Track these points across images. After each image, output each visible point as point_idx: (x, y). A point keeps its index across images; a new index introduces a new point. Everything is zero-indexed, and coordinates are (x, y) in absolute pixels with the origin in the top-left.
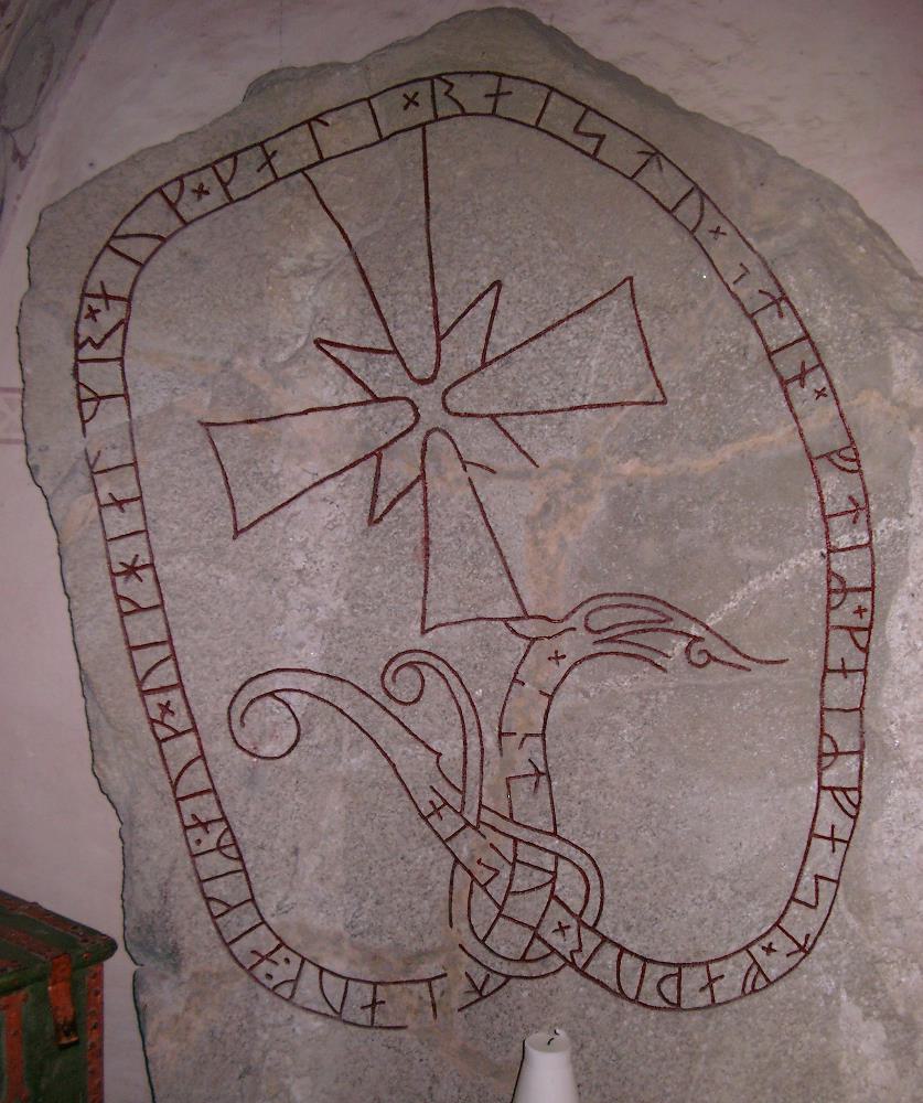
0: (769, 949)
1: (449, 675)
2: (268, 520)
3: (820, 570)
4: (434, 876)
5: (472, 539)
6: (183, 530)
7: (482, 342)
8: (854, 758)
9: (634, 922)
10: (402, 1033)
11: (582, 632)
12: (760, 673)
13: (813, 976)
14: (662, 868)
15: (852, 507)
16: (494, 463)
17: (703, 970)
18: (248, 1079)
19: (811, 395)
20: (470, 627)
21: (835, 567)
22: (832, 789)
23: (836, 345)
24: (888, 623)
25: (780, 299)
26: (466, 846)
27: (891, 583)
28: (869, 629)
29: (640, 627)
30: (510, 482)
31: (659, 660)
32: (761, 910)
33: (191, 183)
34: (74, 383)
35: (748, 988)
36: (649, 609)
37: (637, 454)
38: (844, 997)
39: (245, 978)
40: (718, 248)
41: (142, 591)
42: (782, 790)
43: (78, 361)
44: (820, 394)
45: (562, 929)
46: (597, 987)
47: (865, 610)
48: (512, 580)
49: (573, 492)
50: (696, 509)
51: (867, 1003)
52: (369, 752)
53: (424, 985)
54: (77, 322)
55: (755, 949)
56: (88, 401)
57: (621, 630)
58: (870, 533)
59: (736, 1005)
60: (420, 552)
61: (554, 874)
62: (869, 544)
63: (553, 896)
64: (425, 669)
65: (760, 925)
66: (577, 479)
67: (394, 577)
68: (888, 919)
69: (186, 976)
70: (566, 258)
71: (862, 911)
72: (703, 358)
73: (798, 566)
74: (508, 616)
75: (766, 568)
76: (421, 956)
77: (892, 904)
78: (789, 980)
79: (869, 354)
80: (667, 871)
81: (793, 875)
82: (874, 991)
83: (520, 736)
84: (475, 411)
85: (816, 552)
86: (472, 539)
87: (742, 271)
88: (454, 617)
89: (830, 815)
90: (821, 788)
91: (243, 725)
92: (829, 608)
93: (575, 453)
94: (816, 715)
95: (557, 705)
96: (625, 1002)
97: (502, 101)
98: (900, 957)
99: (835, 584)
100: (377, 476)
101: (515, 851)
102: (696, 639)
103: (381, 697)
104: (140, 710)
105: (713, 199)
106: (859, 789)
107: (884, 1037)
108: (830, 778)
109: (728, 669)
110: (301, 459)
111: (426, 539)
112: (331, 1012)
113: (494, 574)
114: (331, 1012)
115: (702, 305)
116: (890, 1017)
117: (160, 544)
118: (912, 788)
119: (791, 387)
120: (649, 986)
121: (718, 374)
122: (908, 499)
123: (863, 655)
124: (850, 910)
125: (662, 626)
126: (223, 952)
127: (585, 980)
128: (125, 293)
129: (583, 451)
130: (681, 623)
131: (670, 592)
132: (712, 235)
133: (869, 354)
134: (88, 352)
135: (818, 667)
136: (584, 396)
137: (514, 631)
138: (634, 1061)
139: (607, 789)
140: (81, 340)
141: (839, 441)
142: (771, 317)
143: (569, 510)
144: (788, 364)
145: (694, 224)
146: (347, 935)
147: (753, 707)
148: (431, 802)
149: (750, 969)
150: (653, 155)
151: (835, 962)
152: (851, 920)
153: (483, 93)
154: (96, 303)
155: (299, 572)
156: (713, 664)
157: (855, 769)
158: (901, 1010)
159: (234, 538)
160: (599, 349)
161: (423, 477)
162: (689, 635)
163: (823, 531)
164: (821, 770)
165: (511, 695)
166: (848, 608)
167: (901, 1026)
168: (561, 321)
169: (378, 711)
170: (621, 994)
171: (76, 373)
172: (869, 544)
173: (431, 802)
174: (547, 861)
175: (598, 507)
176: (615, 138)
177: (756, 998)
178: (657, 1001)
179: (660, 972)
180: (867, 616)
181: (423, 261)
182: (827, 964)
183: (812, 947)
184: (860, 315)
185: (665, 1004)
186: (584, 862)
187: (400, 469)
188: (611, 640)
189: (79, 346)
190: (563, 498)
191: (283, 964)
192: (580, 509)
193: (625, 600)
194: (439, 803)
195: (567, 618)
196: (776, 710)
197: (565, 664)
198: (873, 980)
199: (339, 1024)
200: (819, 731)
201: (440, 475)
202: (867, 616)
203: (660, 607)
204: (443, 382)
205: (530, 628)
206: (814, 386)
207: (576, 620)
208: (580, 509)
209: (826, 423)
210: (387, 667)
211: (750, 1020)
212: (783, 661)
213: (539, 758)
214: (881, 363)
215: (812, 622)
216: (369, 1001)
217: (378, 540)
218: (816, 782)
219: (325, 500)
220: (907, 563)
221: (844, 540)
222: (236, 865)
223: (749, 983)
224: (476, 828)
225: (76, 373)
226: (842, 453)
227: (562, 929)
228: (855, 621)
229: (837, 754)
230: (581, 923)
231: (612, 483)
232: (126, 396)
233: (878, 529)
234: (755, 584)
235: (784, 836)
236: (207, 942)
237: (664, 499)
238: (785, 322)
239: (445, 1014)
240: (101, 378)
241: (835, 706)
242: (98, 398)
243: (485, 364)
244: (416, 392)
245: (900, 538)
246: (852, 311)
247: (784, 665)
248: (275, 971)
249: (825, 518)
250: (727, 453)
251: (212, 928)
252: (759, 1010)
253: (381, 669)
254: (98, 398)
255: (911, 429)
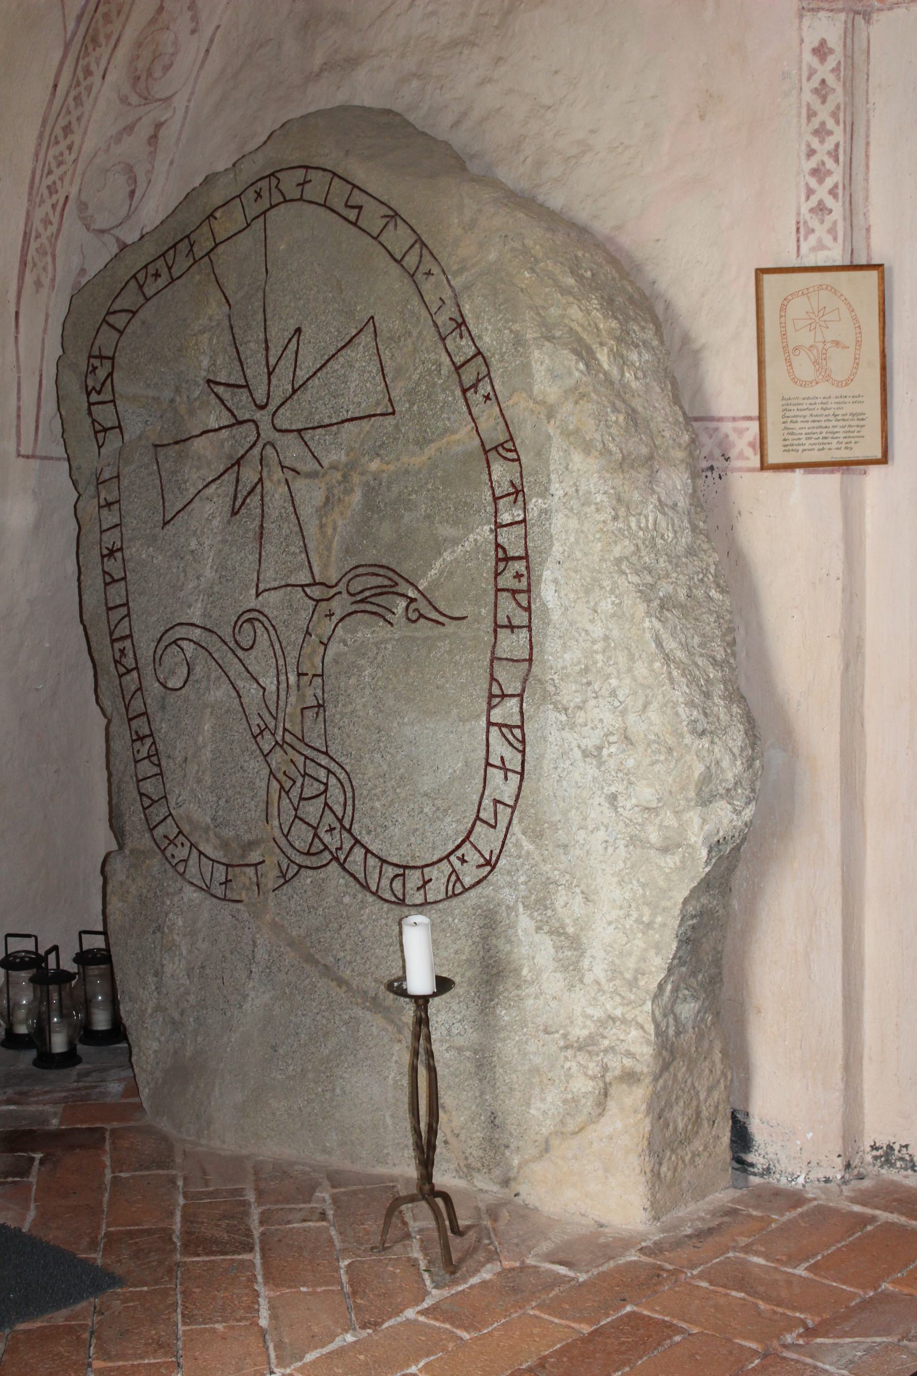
0: (463, 860)
1: (270, 628)
2: (181, 515)
3: (490, 543)
4: (258, 783)
5: (286, 525)
6: (137, 523)
7: (291, 375)
8: (515, 701)
9: (372, 827)
10: (239, 906)
11: (345, 595)
12: (451, 627)
13: (498, 889)
14: (389, 785)
15: (512, 490)
16: (299, 466)
17: (418, 873)
18: (159, 935)
19: (481, 399)
20: (283, 590)
21: (500, 540)
22: (500, 726)
23: (497, 357)
24: (543, 586)
25: (461, 324)
26: (277, 758)
27: (541, 553)
28: (529, 591)
29: (379, 591)
30: (307, 481)
31: (389, 616)
32: (454, 825)
33: (151, 270)
34: (90, 420)
35: (450, 893)
36: (385, 577)
37: (378, 455)
38: (521, 909)
39: (160, 856)
40: (427, 287)
41: (115, 567)
42: (461, 723)
43: (90, 404)
44: (487, 398)
45: (331, 829)
46: (351, 879)
47: (522, 575)
48: (307, 556)
49: (342, 487)
50: (414, 496)
51: (539, 918)
52: (226, 686)
53: (253, 868)
54: (86, 377)
55: (453, 858)
56: (100, 431)
57: (367, 593)
58: (525, 509)
59: (440, 906)
60: (258, 536)
61: (326, 784)
62: (524, 521)
63: (326, 804)
64: (257, 624)
65: (454, 838)
66: (345, 476)
67: (242, 554)
68: (559, 846)
69: (127, 852)
70: (336, 306)
71: (537, 836)
72: (416, 377)
73: (476, 540)
74: (303, 583)
75: (456, 542)
76: (251, 845)
77: (560, 832)
78: (479, 889)
79: (518, 362)
80: (393, 787)
81: (476, 798)
82: (546, 908)
83: (310, 676)
84: (289, 428)
85: (487, 528)
86: (286, 525)
87: (440, 303)
88: (276, 584)
89: (499, 748)
90: (490, 724)
91: (160, 664)
92: (497, 574)
93: (344, 458)
94: (487, 663)
95: (331, 652)
96: (368, 894)
97: (307, 187)
98: (567, 881)
99: (501, 555)
100: (238, 481)
101: (305, 766)
102: (413, 600)
103: (232, 644)
104: (110, 653)
105: (431, 247)
106: (521, 727)
107: (552, 951)
108: (497, 715)
109: (430, 624)
110: (198, 468)
111: (262, 527)
112: (205, 887)
113: (298, 551)
114: (205, 887)
115: (415, 334)
116: (560, 935)
117: (128, 534)
118: (567, 729)
119: (468, 394)
120: (385, 882)
121: (424, 388)
122: (549, 481)
123: (526, 614)
124: (524, 833)
125: (391, 590)
126: (147, 835)
127: (343, 873)
128: (110, 354)
129: (348, 455)
130: (403, 587)
131: (398, 563)
132: (425, 277)
133: (518, 362)
134: (94, 397)
135: (488, 625)
136: (347, 411)
137: (307, 595)
138: (373, 944)
139: (356, 719)
140: (89, 389)
141: (502, 437)
142: (454, 339)
143: (339, 500)
144: (468, 377)
145: (413, 269)
146: (212, 826)
147: (443, 655)
148: (258, 725)
149: (450, 876)
150: (392, 217)
151: (515, 878)
152: (527, 846)
153: (294, 184)
154: (96, 363)
155: (193, 551)
156: (422, 620)
157: (516, 709)
158: (570, 930)
159: (163, 528)
160: (355, 375)
161: (261, 480)
162: (407, 597)
163: (493, 511)
164: (490, 707)
165: (305, 645)
166: (508, 575)
167: (567, 943)
168: (333, 356)
169: (230, 655)
170: (366, 887)
171: (90, 413)
172: (524, 521)
173: (258, 725)
174: (322, 775)
175: (357, 497)
176: (370, 206)
177: (455, 901)
178: (388, 895)
179: (390, 871)
180: (524, 580)
181: (260, 316)
182: (508, 879)
183: (497, 862)
184: (511, 331)
185: (393, 899)
186: (342, 776)
187: (249, 475)
188: (362, 601)
189: (88, 394)
190: (336, 491)
191: (180, 846)
192: (346, 499)
193: (371, 570)
194: (263, 727)
195: (336, 585)
196: (458, 657)
197: (335, 619)
198: (545, 898)
199: (208, 896)
200: (488, 676)
201: (270, 477)
202: (524, 580)
203: (391, 574)
204: (272, 407)
205: (316, 592)
206: (483, 392)
207: (342, 587)
208: (346, 499)
209: (492, 422)
210: (236, 622)
211: (450, 920)
212: (464, 618)
213: (319, 693)
214: (526, 368)
215: (484, 585)
216: (223, 880)
217: (235, 527)
218: (484, 719)
219: (208, 498)
220: (551, 536)
221: (506, 518)
222: (156, 770)
223: (450, 888)
224: (281, 746)
225: (90, 413)
226: (505, 445)
227: (331, 829)
228: (515, 585)
229: (503, 696)
230: (343, 827)
231: (364, 478)
232: (120, 427)
233: (530, 506)
234: (447, 556)
235: (467, 764)
236: (139, 828)
237: (395, 489)
238: (463, 343)
239: (264, 893)
240: (106, 416)
241: (504, 656)
242: (105, 430)
243: (294, 391)
244: (258, 416)
245: (545, 512)
246: (505, 328)
247: (465, 621)
248: (176, 852)
249: (496, 499)
250: (431, 450)
251: (142, 816)
252: (456, 912)
253: (233, 624)
254: (105, 430)
255: (549, 422)
